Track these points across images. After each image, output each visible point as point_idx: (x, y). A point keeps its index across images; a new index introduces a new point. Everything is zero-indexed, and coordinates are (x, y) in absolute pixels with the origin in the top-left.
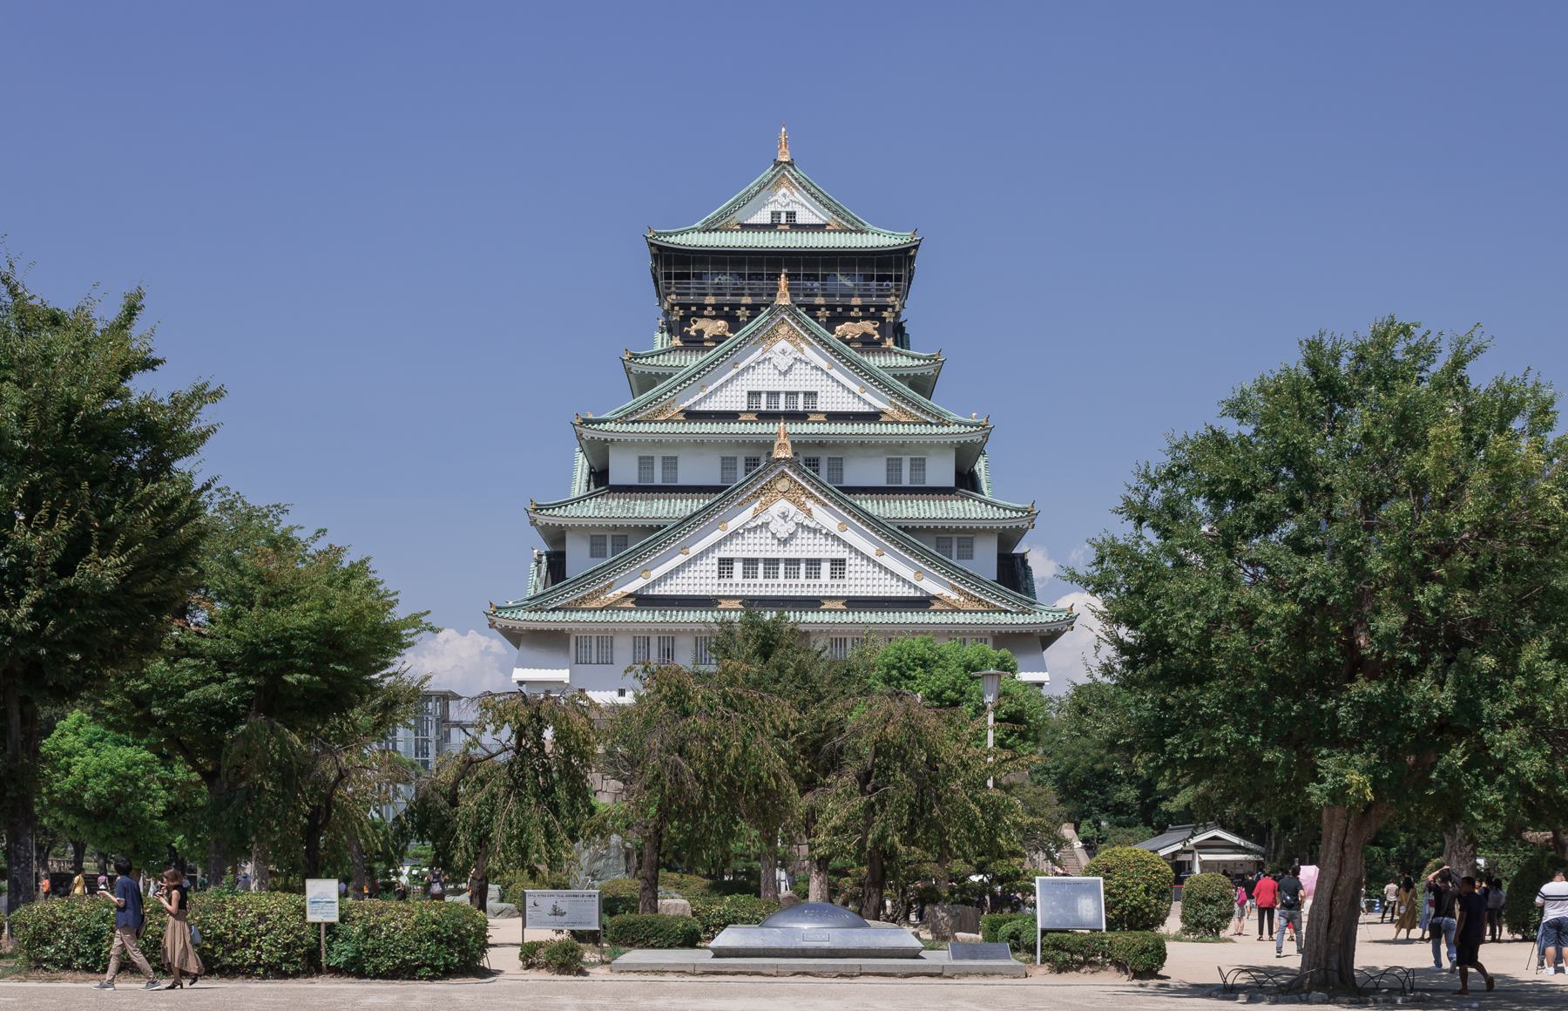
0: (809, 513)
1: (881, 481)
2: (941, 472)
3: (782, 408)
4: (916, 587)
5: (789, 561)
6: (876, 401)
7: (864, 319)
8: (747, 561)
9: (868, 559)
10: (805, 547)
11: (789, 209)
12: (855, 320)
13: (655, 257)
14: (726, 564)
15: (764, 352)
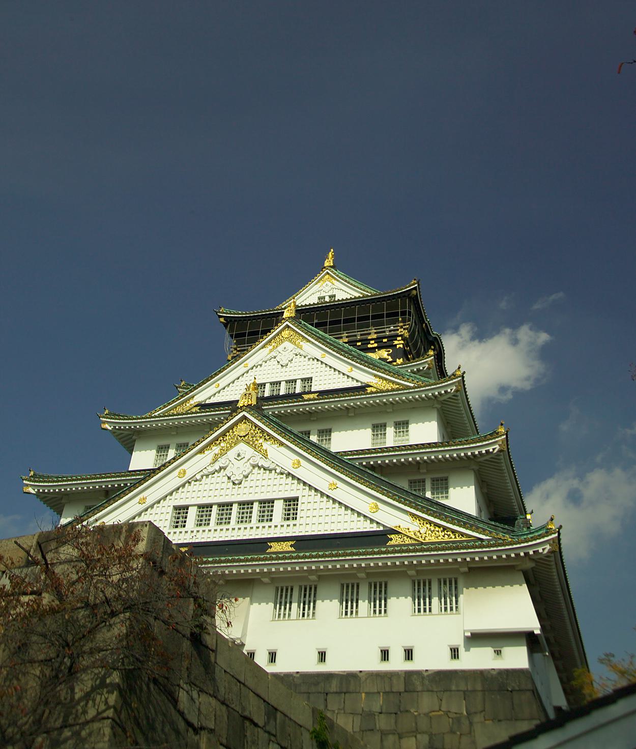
0: (265, 455)
1: (368, 446)
2: (425, 431)
3: (282, 393)
4: (372, 521)
5: (241, 504)
6: (363, 376)
7: (379, 348)
8: (200, 506)
9: (322, 494)
10: (259, 487)
11: (330, 293)
12: (373, 350)
13: (226, 325)
14: (181, 511)
15: (271, 351)
